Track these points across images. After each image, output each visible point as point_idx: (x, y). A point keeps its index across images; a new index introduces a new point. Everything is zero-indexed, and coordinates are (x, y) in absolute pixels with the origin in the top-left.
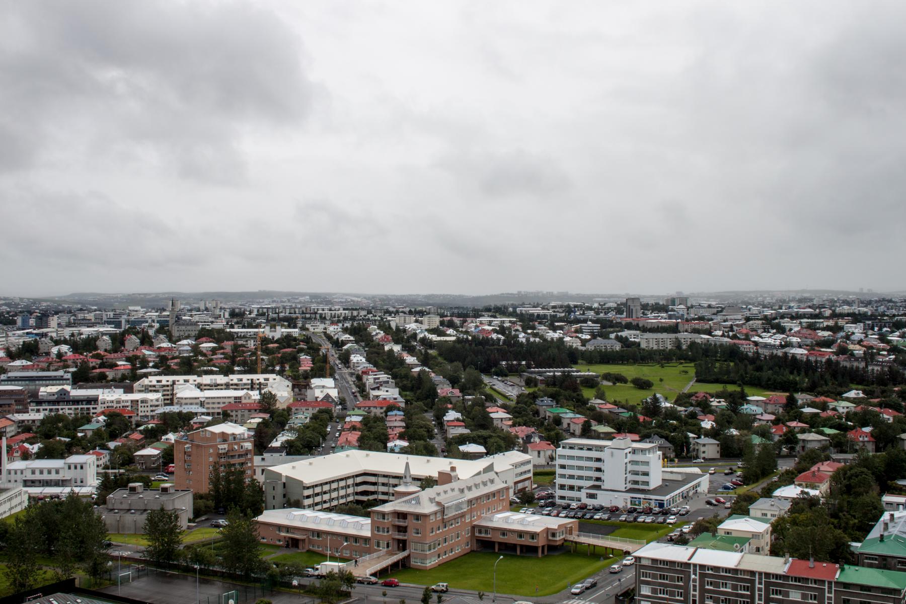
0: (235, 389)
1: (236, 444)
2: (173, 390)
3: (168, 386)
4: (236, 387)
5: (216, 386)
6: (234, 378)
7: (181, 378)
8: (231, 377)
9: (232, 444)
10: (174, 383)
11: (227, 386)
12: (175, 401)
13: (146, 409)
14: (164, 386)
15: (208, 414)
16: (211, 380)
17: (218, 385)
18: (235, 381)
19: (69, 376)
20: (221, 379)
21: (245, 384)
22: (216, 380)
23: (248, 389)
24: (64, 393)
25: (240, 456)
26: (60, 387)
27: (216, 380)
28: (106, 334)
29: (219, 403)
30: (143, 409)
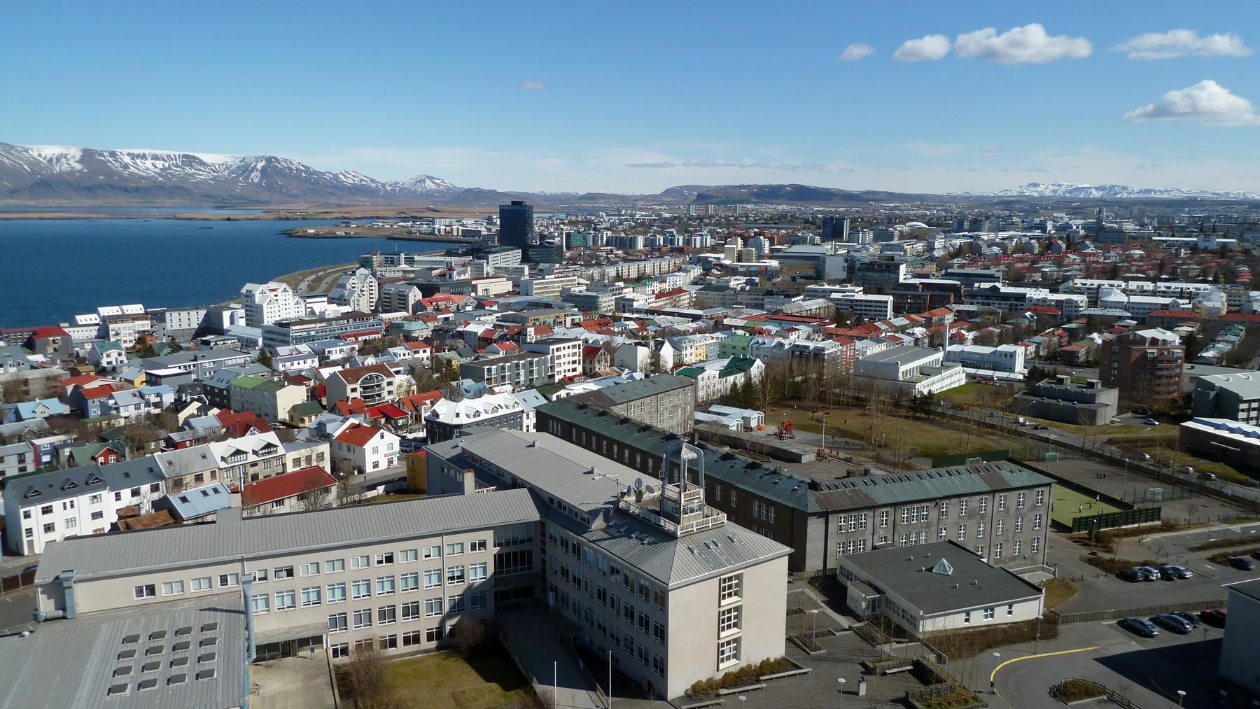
0: (1163, 297)
1: (1166, 349)
2: (1098, 293)
3: (1093, 289)
4: (1164, 294)
5: (1143, 292)
6: (1162, 286)
7: (1106, 283)
8: (1159, 284)
9: (1162, 350)
10: (1099, 286)
11: (1154, 293)
12: (1099, 303)
13: (1070, 309)
14: (1089, 289)
15: (1132, 318)
16: (1138, 286)
17: (1145, 291)
18: (1163, 289)
19: (1000, 275)
20: (1149, 286)
21: (1174, 292)
22: (1142, 286)
23: (1177, 297)
24: (995, 289)
25: (1168, 361)
26: (992, 284)
27: (1142, 286)
28: (1034, 239)
29: (1144, 309)
30: (1068, 309)
